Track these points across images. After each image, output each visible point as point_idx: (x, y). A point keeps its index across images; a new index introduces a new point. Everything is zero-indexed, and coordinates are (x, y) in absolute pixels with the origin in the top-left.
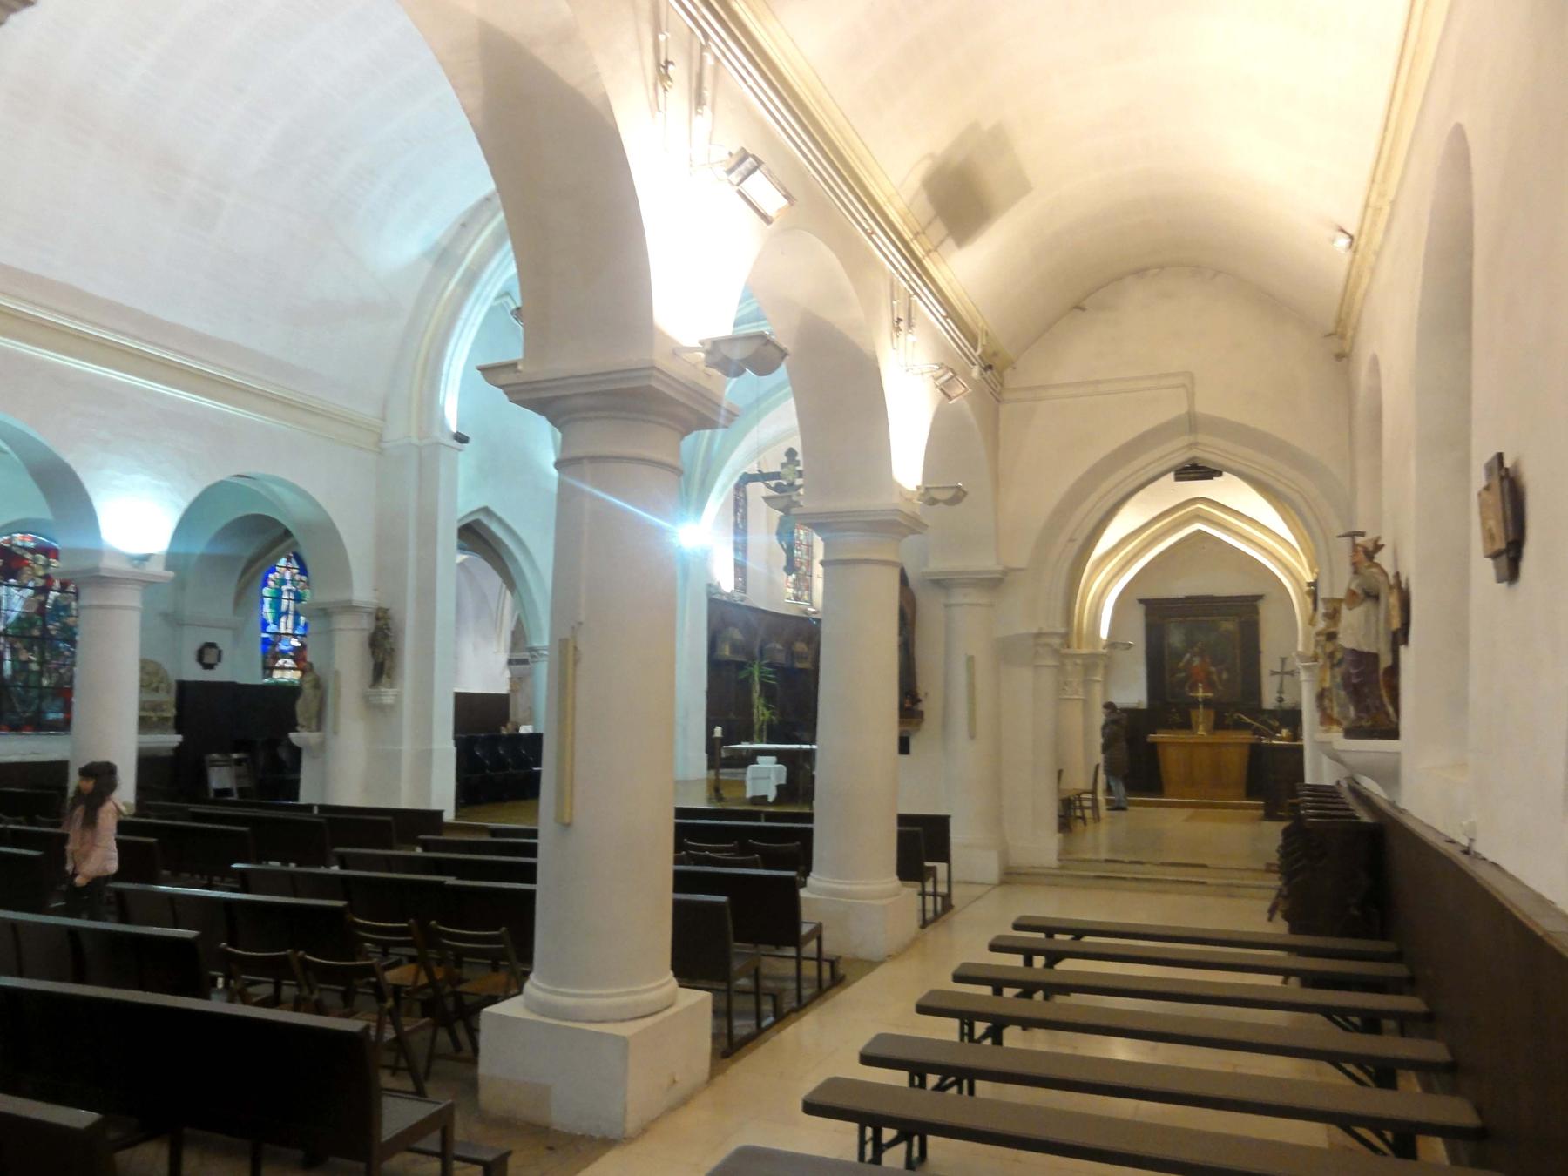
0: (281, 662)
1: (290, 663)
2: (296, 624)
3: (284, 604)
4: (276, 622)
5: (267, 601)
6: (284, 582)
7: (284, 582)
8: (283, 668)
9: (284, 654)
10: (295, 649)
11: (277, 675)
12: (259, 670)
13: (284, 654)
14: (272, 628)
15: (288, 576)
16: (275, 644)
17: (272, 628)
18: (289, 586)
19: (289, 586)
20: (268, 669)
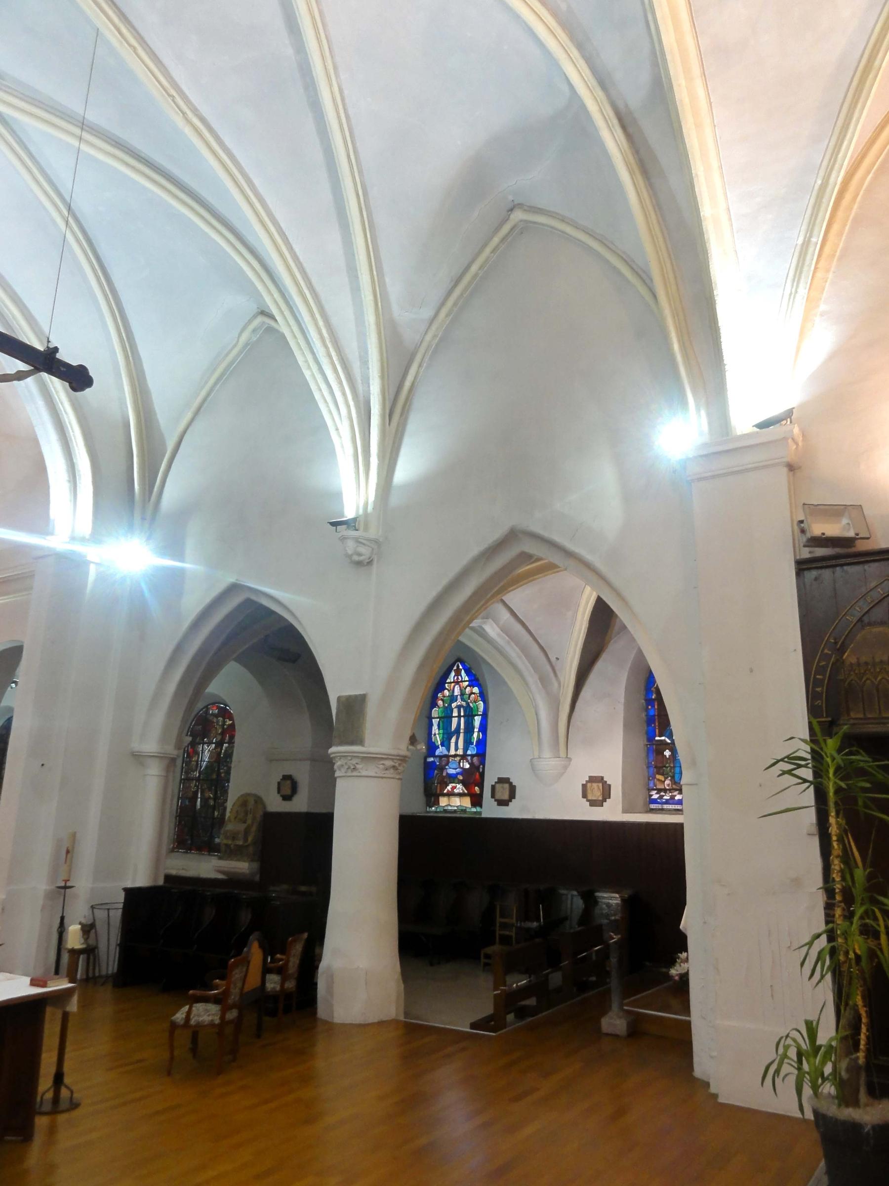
0: (449, 788)
1: (459, 788)
2: (468, 743)
3: (455, 721)
4: (446, 743)
5: (435, 722)
6: (453, 699)
7: (453, 699)
8: (451, 794)
9: (452, 778)
10: (464, 772)
11: (443, 801)
12: (420, 798)
13: (452, 778)
14: (441, 751)
15: (457, 692)
16: (442, 768)
17: (441, 751)
18: (459, 702)
19: (459, 702)
20: (432, 795)
